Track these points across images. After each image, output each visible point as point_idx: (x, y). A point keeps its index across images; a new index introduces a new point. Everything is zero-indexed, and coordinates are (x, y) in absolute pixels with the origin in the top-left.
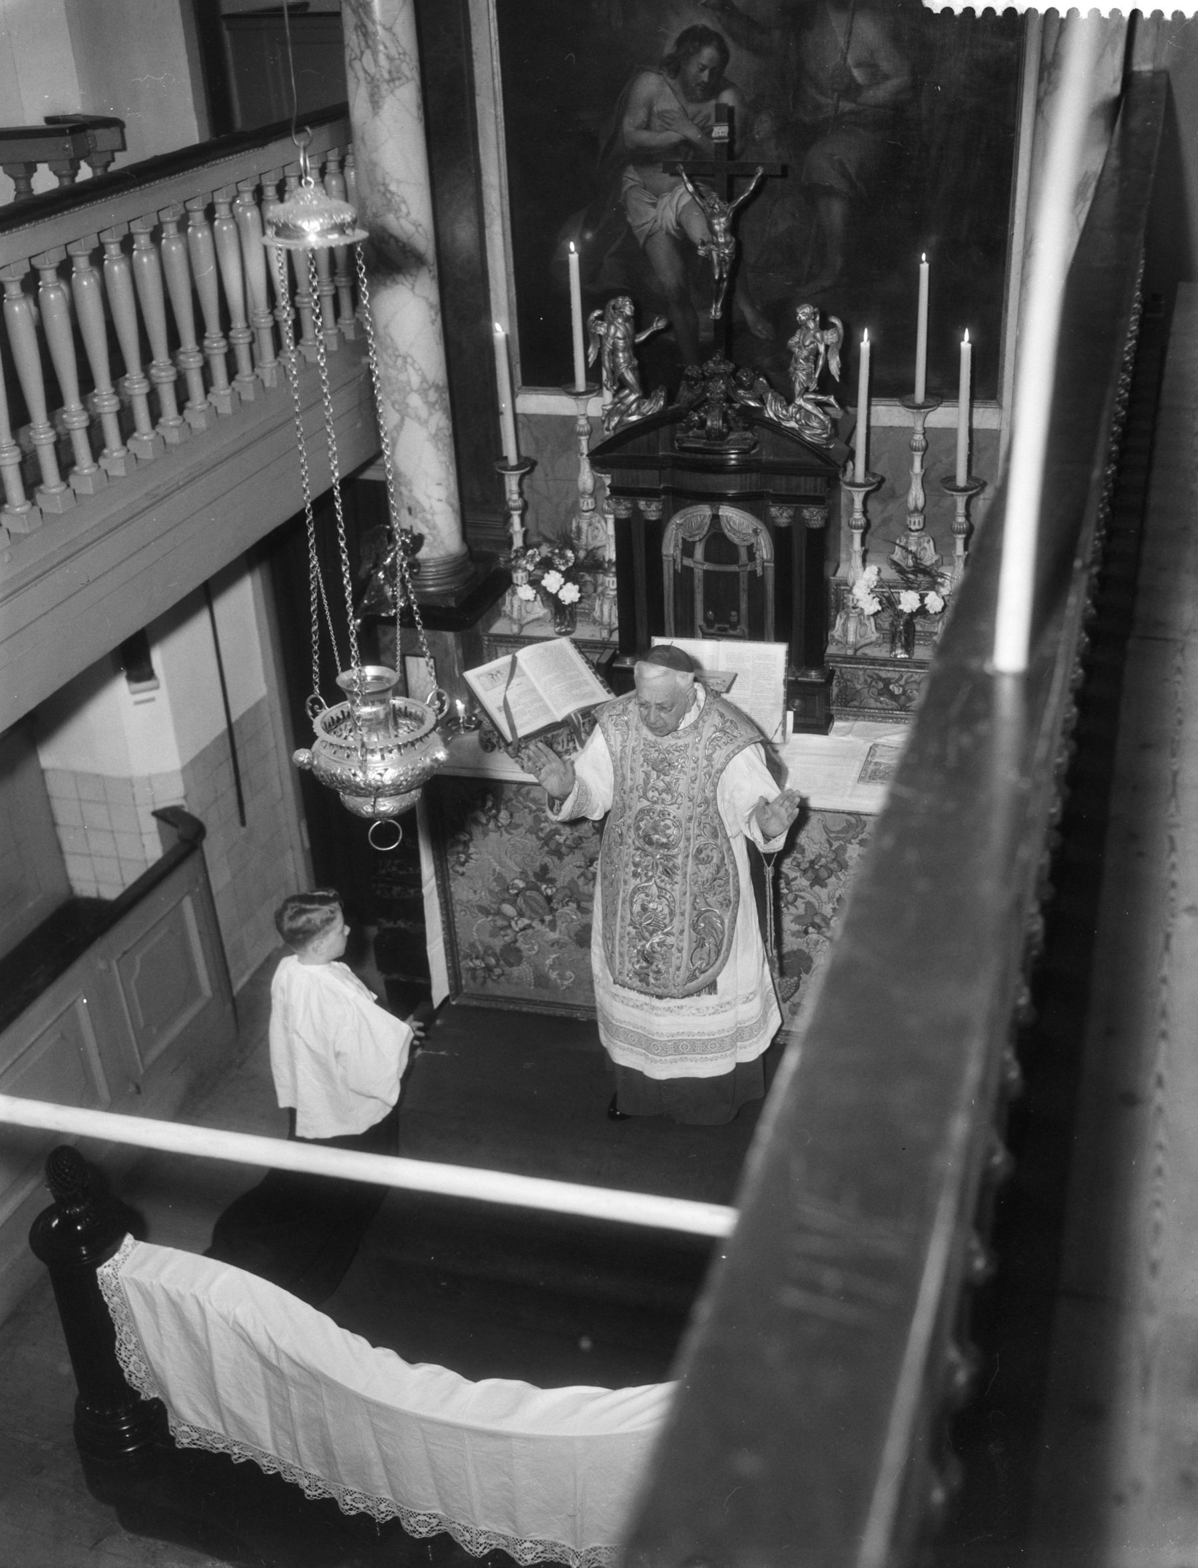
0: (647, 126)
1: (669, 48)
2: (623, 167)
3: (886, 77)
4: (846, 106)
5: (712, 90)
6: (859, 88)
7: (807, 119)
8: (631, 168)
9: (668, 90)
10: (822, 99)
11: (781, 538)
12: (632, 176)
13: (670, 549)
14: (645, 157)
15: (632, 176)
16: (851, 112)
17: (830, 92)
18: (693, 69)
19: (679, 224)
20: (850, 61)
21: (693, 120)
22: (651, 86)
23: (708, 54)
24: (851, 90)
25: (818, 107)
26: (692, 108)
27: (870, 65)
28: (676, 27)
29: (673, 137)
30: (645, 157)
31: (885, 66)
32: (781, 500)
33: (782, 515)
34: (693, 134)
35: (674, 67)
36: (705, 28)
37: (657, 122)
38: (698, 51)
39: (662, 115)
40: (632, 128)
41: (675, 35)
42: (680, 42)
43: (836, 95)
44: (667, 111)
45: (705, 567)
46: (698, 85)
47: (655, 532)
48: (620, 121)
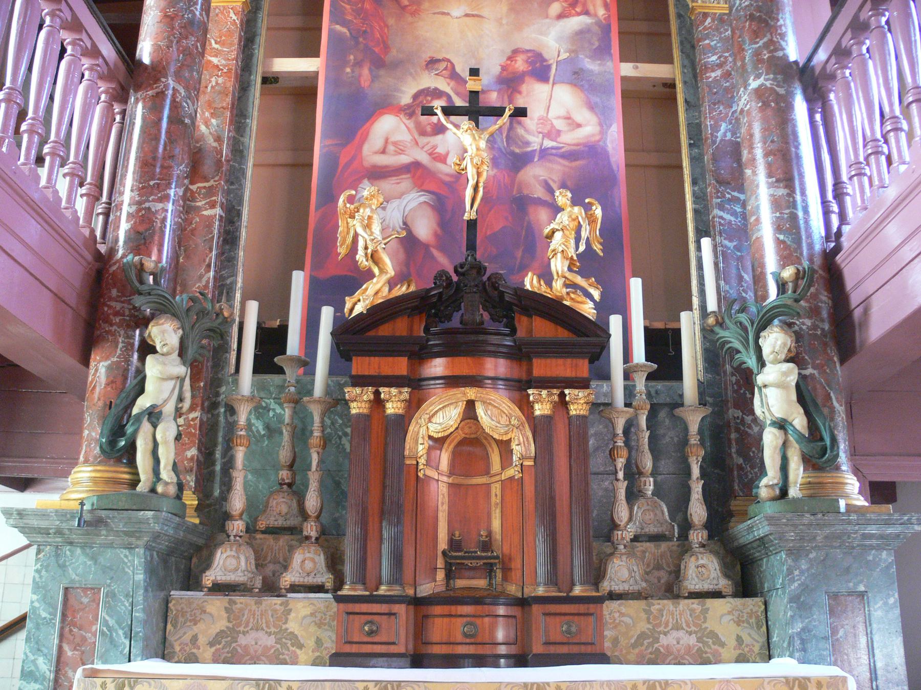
3: (579, 126)
4: (548, 143)
6: (559, 132)
7: (517, 151)
8: (366, 181)
9: (404, 127)
10: (531, 138)
11: (541, 429)
13: (417, 443)
16: (552, 148)
17: (536, 133)
19: (405, 223)
20: (550, 115)
21: (423, 147)
22: (387, 126)
24: (553, 134)
25: (527, 143)
26: (423, 140)
27: (568, 118)
29: (404, 159)
31: (578, 118)
34: (423, 157)
36: (436, 89)
39: (395, 144)
43: (541, 135)
44: (400, 141)
45: (450, 480)
46: (429, 124)
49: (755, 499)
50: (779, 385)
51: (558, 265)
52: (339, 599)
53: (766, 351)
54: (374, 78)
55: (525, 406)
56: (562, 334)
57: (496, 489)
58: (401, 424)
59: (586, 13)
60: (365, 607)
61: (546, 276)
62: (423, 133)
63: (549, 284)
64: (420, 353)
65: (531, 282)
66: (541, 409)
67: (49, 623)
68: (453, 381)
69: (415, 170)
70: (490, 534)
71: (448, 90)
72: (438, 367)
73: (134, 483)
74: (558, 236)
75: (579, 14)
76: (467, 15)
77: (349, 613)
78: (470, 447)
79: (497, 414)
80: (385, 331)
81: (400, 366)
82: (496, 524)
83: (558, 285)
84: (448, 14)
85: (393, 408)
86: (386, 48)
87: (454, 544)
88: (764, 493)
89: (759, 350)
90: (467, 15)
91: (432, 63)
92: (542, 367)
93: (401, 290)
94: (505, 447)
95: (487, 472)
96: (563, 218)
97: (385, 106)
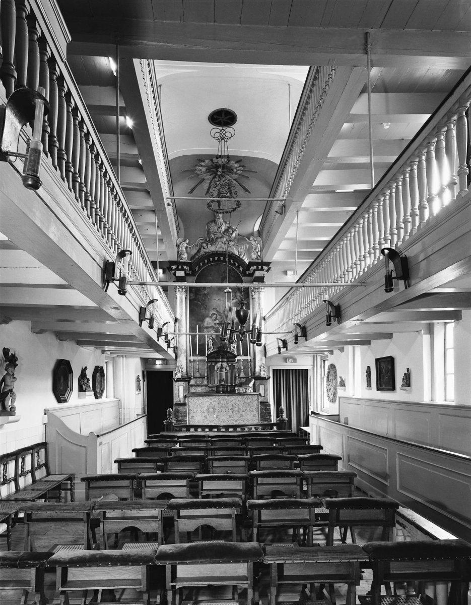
1: (210, 315)
5: (215, 320)
14: (207, 328)
22: (207, 320)
23: (215, 316)
32: (231, 361)
34: (213, 325)
35: (211, 317)
40: (205, 325)
54: (205, 312)
55: (228, 364)
56: (231, 355)
58: (214, 367)
64: (216, 358)
65: (228, 350)
68: (219, 362)
72: (218, 360)
78: (222, 367)
79: (225, 365)
81: (214, 360)
87: (220, 380)
92: (230, 360)
93: (214, 350)
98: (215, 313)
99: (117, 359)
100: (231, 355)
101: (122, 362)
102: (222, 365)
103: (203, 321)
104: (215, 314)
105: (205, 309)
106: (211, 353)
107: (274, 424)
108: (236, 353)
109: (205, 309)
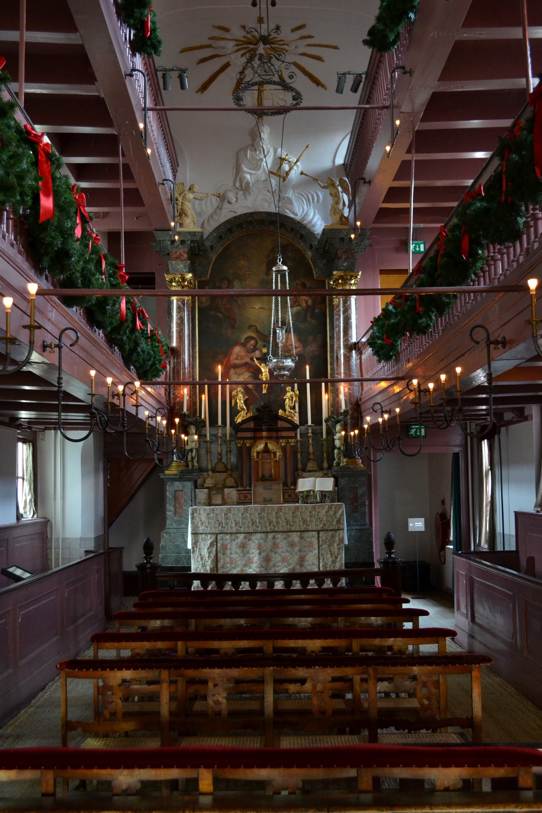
0: (237, 359)
1: (243, 341)
2: (230, 368)
5: (254, 350)
11: (284, 449)
12: (232, 371)
14: (236, 366)
15: (232, 371)
18: (249, 345)
20: (288, 344)
22: (237, 350)
23: (253, 342)
26: (248, 355)
28: (244, 336)
29: (243, 361)
30: (236, 366)
33: (283, 442)
35: (244, 345)
37: (239, 358)
38: (250, 341)
41: (245, 337)
42: (246, 339)
47: (249, 449)
48: (230, 357)
49: (333, 466)
50: (339, 439)
51: (287, 407)
52: (238, 490)
53: (337, 430)
56: (289, 426)
57: (273, 463)
59: (299, 305)
60: (243, 492)
61: (284, 410)
62: (248, 352)
63: (285, 412)
66: (283, 444)
67: (172, 499)
68: (261, 438)
69: (246, 364)
70: (271, 474)
71: (255, 337)
72: (258, 434)
73: (187, 466)
74: (287, 400)
75: (297, 306)
76: (261, 308)
77: (240, 494)
80: (245, 426)
81: (249, 434)
82: (273, 471)
83: (287, 413)
84: (254, 308)
85: (248, 445)
86: (235, 321)
88: (335, 464)
89: (335, 429)
90: (261, 308)
91: (250, 326)
92: (284, 434)
93: (249, 415)
94: (275, 453)
95: (270, 459)
96: (288, 394)
97: (236, 343)
98: (253, 334)
99: (40, 436)
100: (289, 426)
101: (52, 439)
102: (266, 445)
103: (227, 354)
104: (251, 338)
105: (233, 327)
106: (244, 422)
107: (378, 572)
108: (296, 419)
109: (233, 327)
